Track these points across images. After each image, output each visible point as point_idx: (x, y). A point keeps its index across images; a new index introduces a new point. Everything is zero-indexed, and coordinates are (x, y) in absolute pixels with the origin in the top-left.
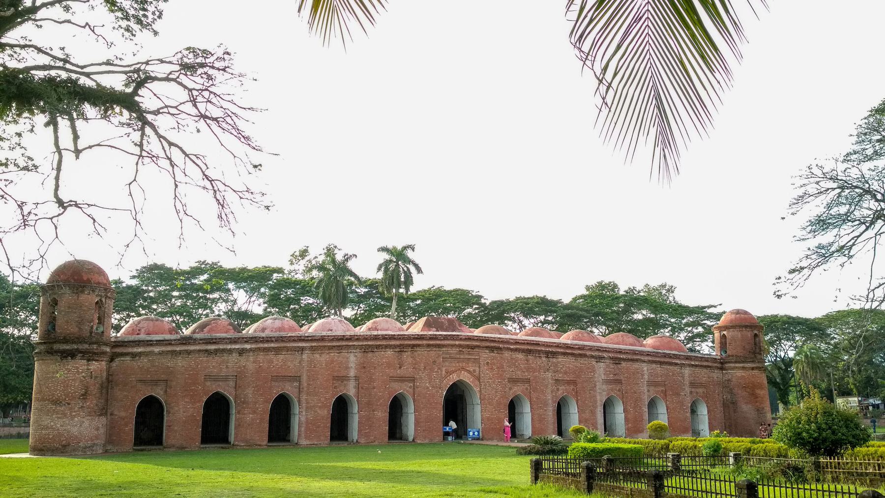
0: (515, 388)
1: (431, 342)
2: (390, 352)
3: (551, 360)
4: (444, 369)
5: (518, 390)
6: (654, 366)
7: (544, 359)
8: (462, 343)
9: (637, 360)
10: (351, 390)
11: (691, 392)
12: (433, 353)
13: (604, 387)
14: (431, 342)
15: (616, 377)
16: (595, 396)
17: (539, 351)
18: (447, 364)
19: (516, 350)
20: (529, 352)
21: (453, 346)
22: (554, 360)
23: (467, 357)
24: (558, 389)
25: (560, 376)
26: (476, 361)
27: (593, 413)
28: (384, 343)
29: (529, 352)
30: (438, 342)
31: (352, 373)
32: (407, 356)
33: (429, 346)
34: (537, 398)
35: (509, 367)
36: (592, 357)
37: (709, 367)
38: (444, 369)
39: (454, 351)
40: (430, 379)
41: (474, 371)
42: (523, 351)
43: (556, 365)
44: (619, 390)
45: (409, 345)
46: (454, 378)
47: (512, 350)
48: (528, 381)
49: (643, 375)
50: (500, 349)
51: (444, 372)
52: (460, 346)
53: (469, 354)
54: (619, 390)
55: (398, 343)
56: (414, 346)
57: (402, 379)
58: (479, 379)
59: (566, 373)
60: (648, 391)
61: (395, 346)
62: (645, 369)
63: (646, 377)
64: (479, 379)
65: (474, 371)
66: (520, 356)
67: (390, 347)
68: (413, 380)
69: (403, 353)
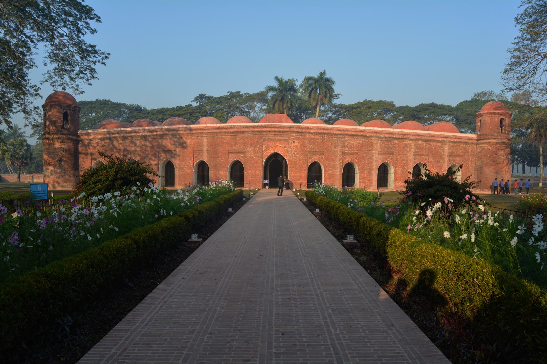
2: (228, 137)
6: (420, 142)
7: (335, 139)
8: (276, 129)
9: (406, 139)
10: (205, 159)
11: (449, 160)
13: (380, 156)
15: (390, 150)
16: (371, 163)
17: (331, 134)
18: (266, 142)
20: (325, 134)
23: (280, 138)
24: (345, 158)
26: (286, 140)
27: (370, 173)
30: (260, 129)
31: (205, 149)
33: (253, 132)
34: (328, 164)
35: (309, 144)
36: (371, 137)
37: (465, 143)
38: (264, 146)
39: (271, 134)
40: (255, 152)
41: (285, 147)
42: (320, 134)
44: (391, 159)
45: (241, 132)
46: (271, 151)
48: (323, 153)
49: (410, 149)
52: (275, 131)
53: (281, 136)
54: (391, 159)
56: (243, 132)
57: (237, 152)
59: (351, 147)
60: (415, 159)
62: (413, 144)
63: (413, 150)
65: (285, 147)
67: (229, 133)
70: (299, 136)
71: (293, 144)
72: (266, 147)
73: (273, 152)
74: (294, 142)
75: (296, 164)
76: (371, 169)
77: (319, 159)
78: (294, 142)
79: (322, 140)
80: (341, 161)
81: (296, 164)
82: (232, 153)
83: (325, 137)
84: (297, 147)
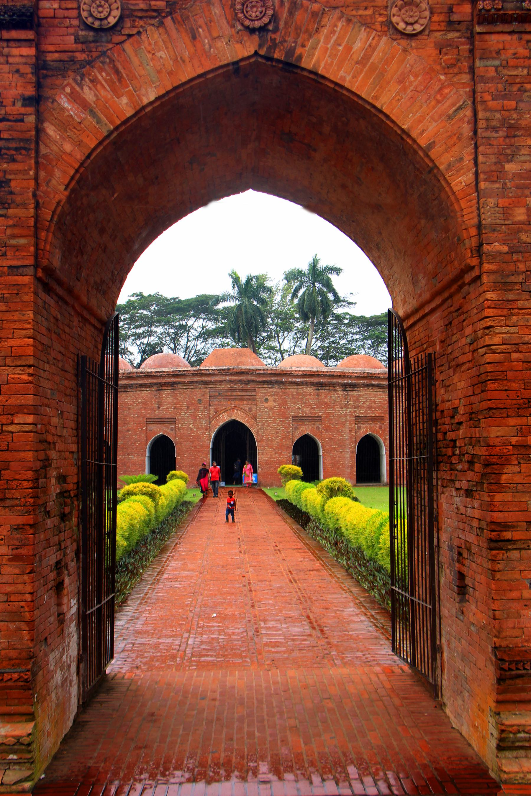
0: (303, 428)
1: (196, 379)
2: (146, 392)
3: (351, 393)
4: (212, 408)
5: (306, 429)
7: (341, 393)
12: (198, 393)
14: (196, 379)
17: (334, 385)
19: (303, 383)
21: (221, 382)
22: (355, 393)
23: (240, 394)
24: (359, 428)
25: (362, 412)
28: (140, 382)
29: (320, 385)
30: (205, 379)
32: (167, 395)
33: (192, 383)
34: (330, 439)
35: (294, 403)
40: (194, 418)
42: (312, 384)
43: (357, 400)
45: (168, 383)
46: (225, 418)
47: (297, 384)
48: (318, 419)
50: (282, 383)
51: (212, 412)
52: (231, 382)
53: (243, 391)
55: (155, 381)
56: (173, 384)
57: (161, 421)
58: (255, 418)
59: (370, 408)
61: (151, 385)
64: (255, 418)
65: (250, 409)
66: (310, 390)
68: (173, 421)
69: (162, 392)
70: (275, 389)
71: (265, 405)
72: (216, 411)
73: (229, 419)
74: (266, 400)
75: (271, 441)
77: (312, 431)
78: (266, 400)
79: (318, 395)
80: (353, 433)
81: (271, 441)
82: (154, 422)
83: (323, 392)
84: (271, 409)
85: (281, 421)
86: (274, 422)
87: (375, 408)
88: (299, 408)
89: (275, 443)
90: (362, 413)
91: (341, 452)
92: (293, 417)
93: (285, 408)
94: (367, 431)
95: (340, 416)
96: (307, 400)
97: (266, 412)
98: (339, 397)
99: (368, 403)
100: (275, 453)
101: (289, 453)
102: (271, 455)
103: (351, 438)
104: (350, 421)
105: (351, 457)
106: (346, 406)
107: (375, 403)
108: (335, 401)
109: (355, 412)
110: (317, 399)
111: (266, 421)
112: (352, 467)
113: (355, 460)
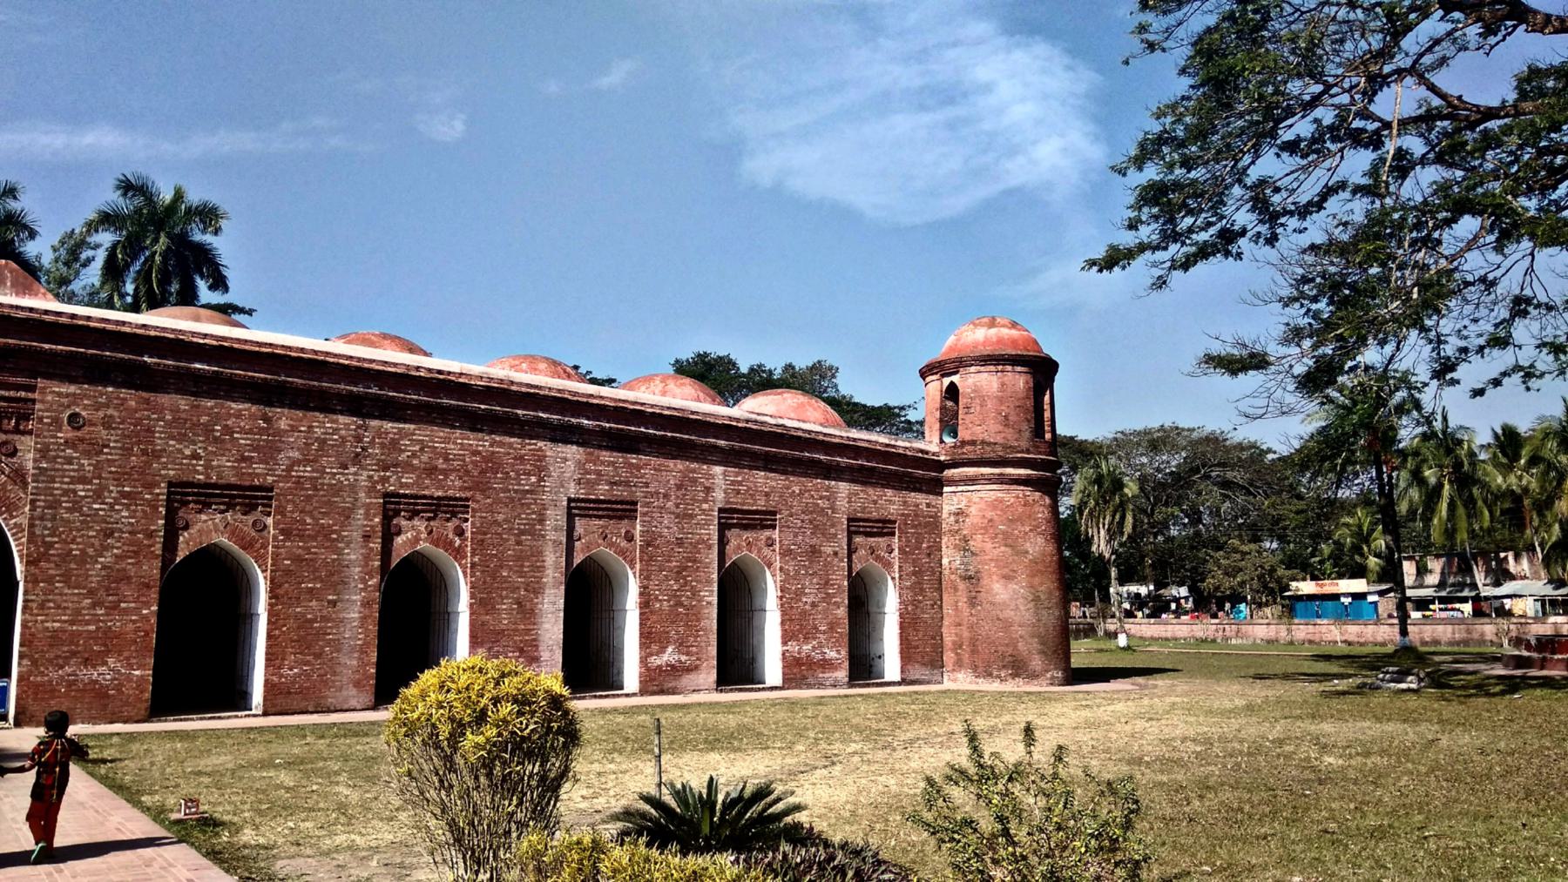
15: (620, 493)
16: (539, 554)
35: (181, 438)
49: (708, 490)
59: (431, 470)
75: (83, 559)
76: (536, 589)
77: (234, 534)
79: (267, 419)
80: (376, 545)
85: (124, 495)
86: (98, 495)
87: (446, 473)
88: (195, 456)
89: (95, 572)
90: (407, 485)
91: (333, 603)
92: (170, 484)
93: (144, 452)
94: (417, 540)
95: (337, 489)
96: (228, 430)
97: (69, 461)
98: (336, 431)
99: (425, 458)
100: (94, 606)
101: (147, 605)
102: (78, 612)
103: (367, 558)
104: (368, 507)
105: (364, 619)
106: (357, 459)
107: (446, 460)
108: (323, 442)
109: (384, 480)
110: (261, 431)
111: (66, 492)
112: (363, 651)
113: (373, 628)
